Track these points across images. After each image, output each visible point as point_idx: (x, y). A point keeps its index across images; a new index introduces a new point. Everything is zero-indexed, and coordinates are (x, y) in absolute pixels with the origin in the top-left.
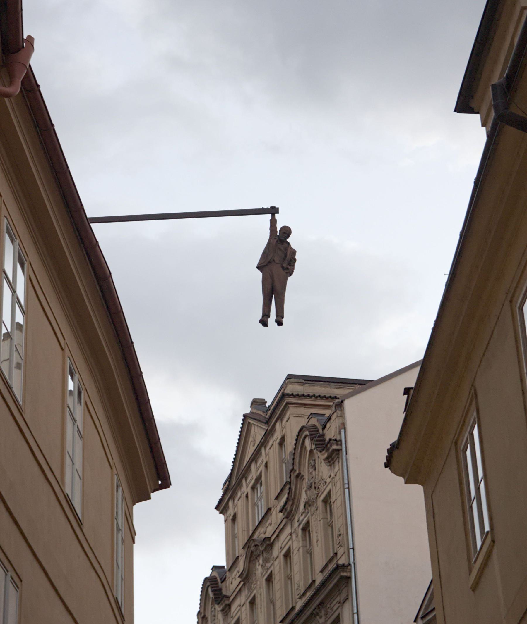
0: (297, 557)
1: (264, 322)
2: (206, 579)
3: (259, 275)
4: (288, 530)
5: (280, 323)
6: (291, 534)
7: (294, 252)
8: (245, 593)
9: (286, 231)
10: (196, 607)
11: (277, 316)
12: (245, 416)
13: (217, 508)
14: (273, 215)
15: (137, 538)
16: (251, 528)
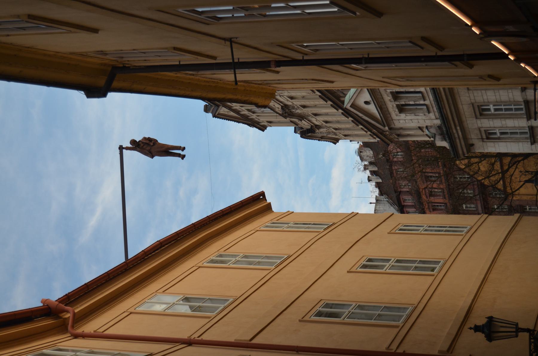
1: (183, 157)
2: (301, 137)
3: (156, 158)
5: (184, 149)
6: (280, 96)
7: (145, 138)
8: (310, 118)
9: (133, 142)
10: (316, 142)
11: (179, 149)
12: (213, 117)
13: (263, 131)
14: (124, 148)
15: (291, 210)
16: (275, 114)
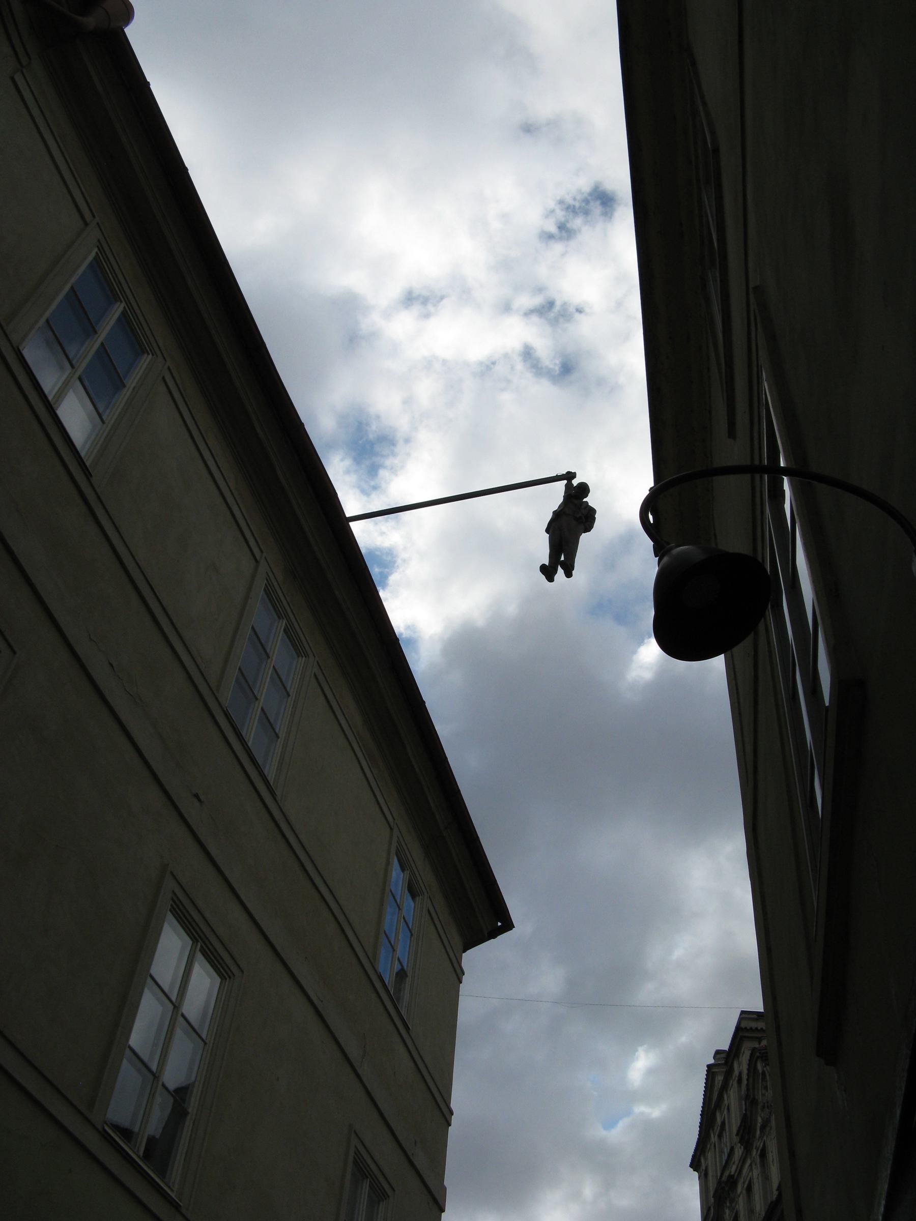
0: (757, 1188)
4: (749, 1162)
6: (751, 1165)
12: (708, 1066)
16: (719, 1175)
